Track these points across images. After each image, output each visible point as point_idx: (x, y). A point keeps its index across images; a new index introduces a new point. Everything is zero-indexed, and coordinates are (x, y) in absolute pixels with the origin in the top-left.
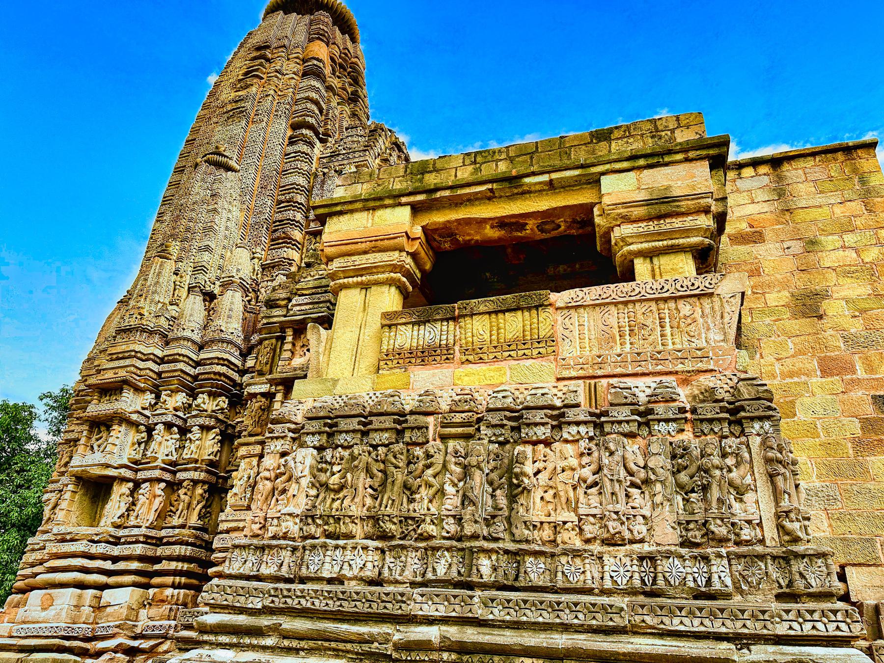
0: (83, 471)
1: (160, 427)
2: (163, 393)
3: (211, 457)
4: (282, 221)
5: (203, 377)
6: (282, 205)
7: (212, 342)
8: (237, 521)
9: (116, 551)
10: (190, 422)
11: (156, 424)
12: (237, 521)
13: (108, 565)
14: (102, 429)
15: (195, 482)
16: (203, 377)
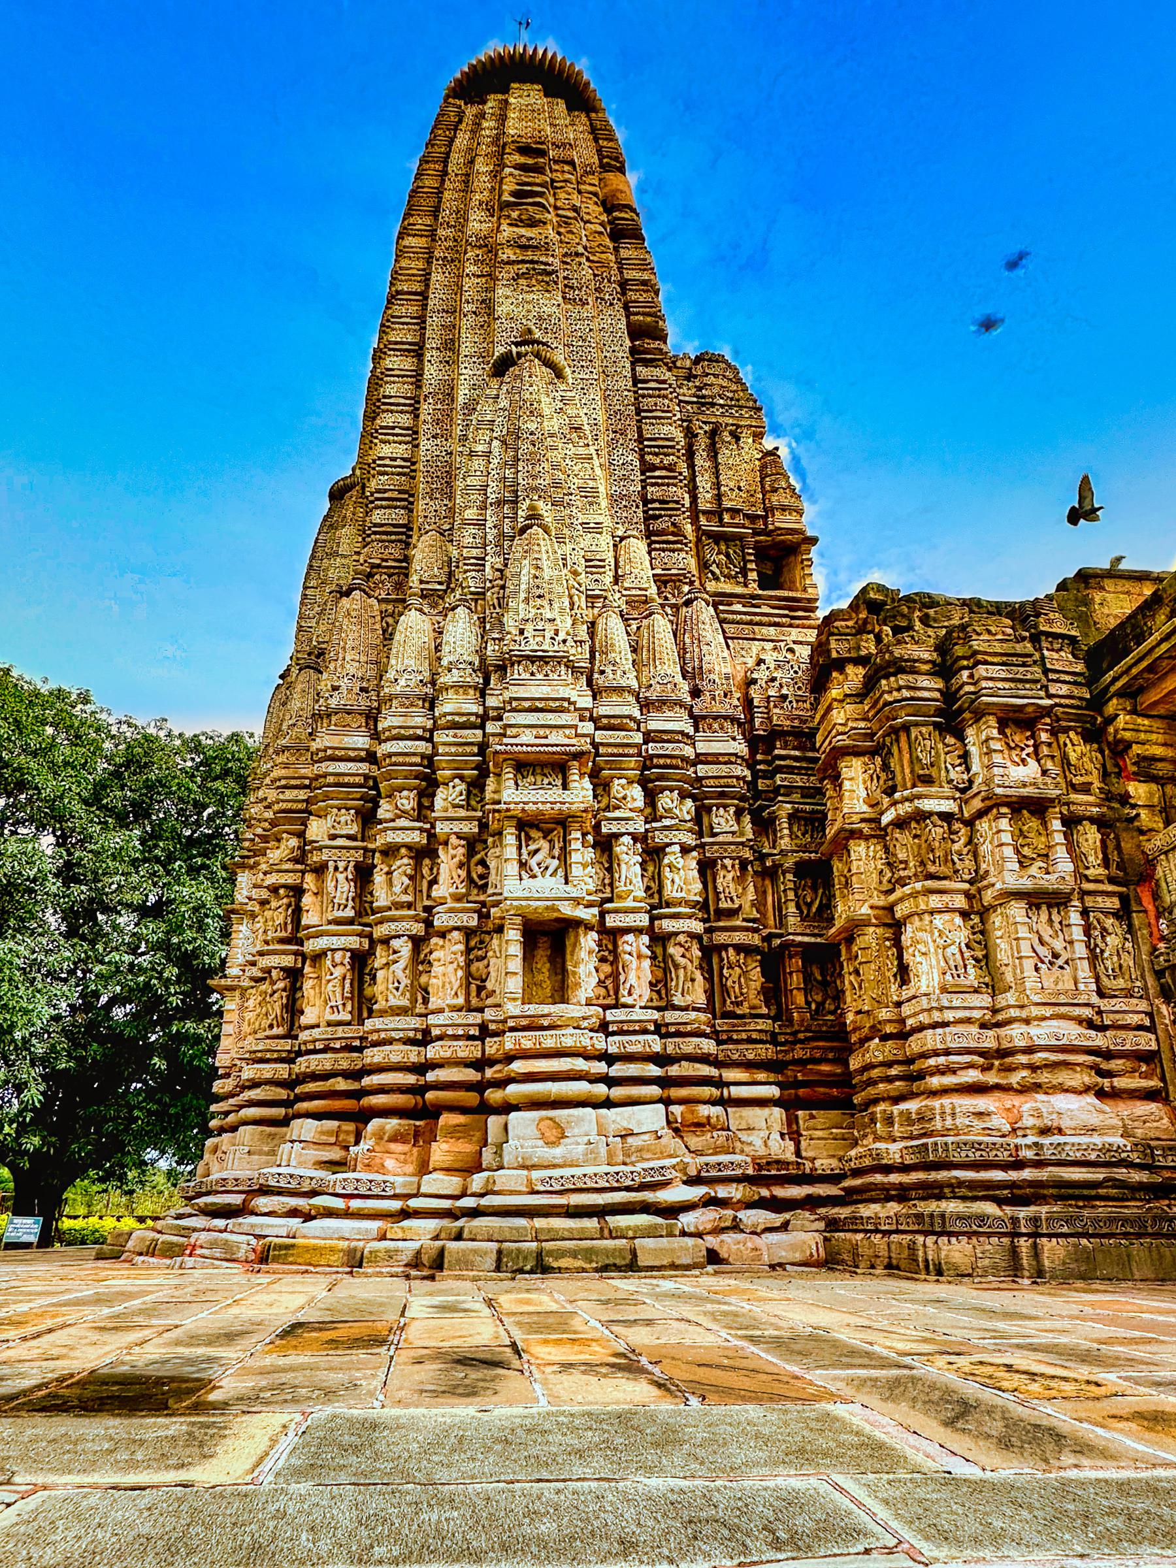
0: (547, 908)
1: (626, 839)
2: (616, 782)
3: (698, 898)
4: (667, 502)
5: (662, 761)
6: (657, 473)
7: (664, 702)
8: (965, 1008)
9: (614, 1045)
10: (660, 838)
11: (622, 834)
12: (965, 1008)
13: (600, 1067)
14: (534, 834)
15: (692, 936)
16: (662, 761)
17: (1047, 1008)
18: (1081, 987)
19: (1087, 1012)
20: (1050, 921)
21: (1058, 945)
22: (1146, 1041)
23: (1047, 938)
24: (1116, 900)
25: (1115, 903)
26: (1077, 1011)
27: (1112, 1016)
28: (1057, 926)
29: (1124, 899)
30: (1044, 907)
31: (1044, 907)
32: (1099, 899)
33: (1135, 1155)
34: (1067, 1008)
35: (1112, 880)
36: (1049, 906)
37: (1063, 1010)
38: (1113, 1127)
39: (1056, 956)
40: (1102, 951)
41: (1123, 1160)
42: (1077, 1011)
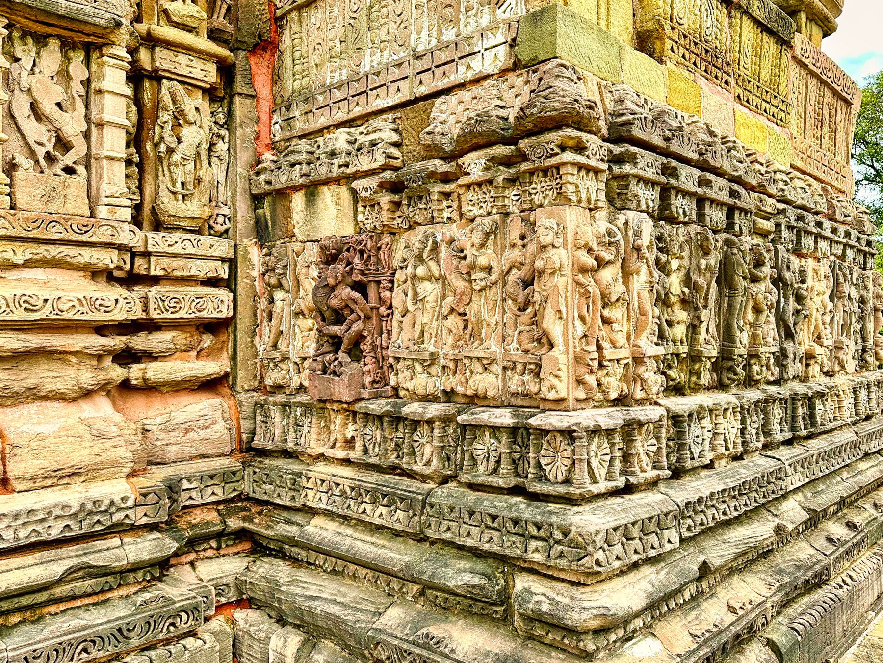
17: (19, 247)
18: (102, 212)
19: (108, 259)
20: (64, 75)
21: (72, 125)
22: (216, 304)
23: (48, 107)
24: (212, 68)
25: (210, 74)
26: (86, 256)
27: (166, 262)
28: (77, 88)
29: (226, 70)
30: (54, 44)
31: (54, 44)
32: (183, 59)
33: (140, 511)
34: (66, 250)
35: (214, 35)
36: (67, 45)
37: (54, 251)
38: (115, 464)
39: (64, 145)
40: (170, 151)
41: (114, 525)
42: (86, 256)
